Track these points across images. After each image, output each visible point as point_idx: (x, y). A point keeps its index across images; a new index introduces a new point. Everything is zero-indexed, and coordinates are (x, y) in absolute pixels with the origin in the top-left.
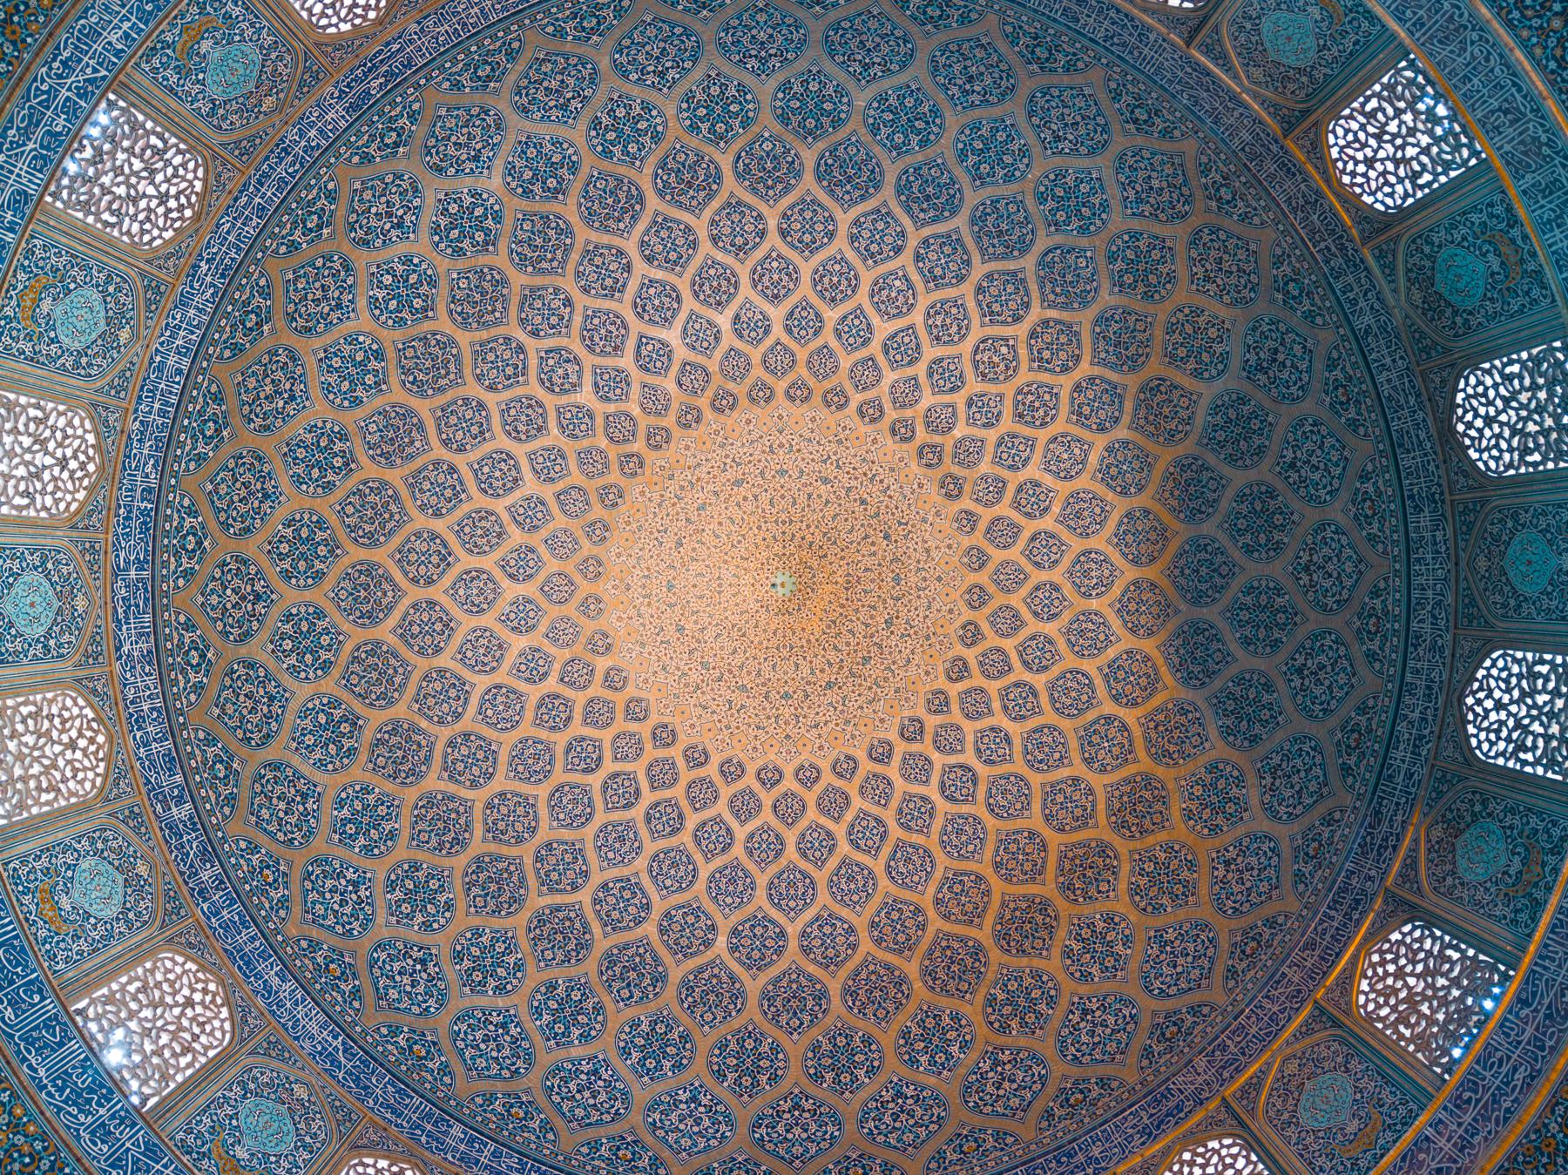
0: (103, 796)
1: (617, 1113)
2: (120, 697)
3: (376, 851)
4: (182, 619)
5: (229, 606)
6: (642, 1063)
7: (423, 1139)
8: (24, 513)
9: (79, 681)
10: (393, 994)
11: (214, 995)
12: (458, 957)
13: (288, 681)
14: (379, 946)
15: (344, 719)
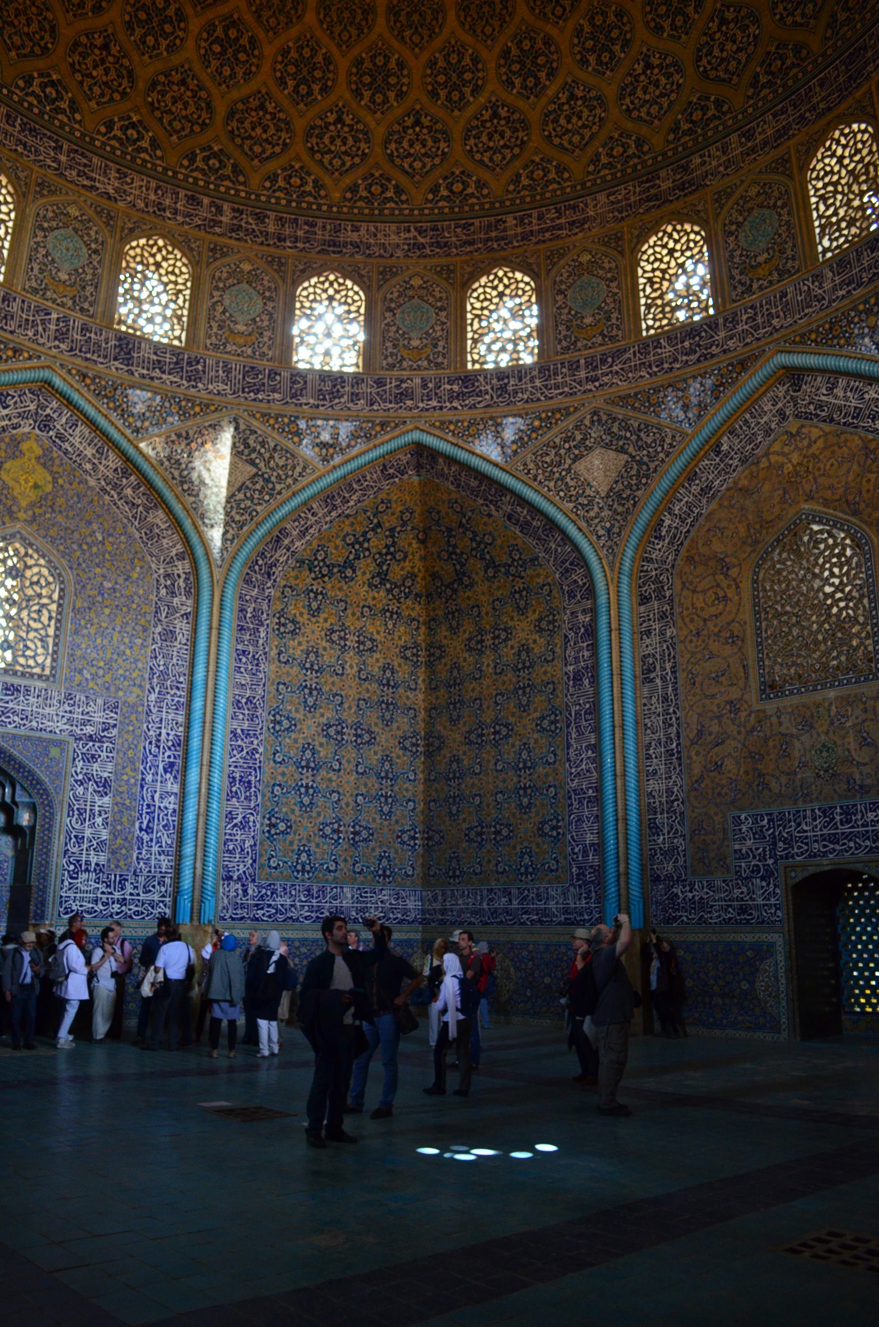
0: (194, 263)
1: (601, 119)
2: (140, 214)
3: (329, 83)
4: (103, 129)
5: (104, 79)
6: (599, 62)
7: (495, 246)
8: (10, 231)
9: (122, 239)
10: (418, 165)
11: (336, 280)
12: (434, 94)
13: (176, 59)
14: (387, 142)
15: (226, 29)
